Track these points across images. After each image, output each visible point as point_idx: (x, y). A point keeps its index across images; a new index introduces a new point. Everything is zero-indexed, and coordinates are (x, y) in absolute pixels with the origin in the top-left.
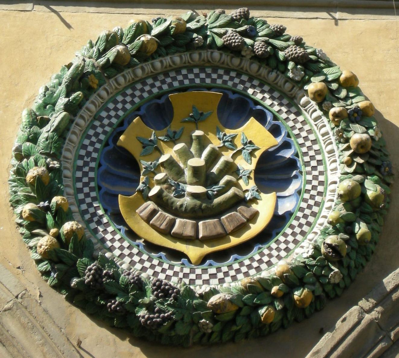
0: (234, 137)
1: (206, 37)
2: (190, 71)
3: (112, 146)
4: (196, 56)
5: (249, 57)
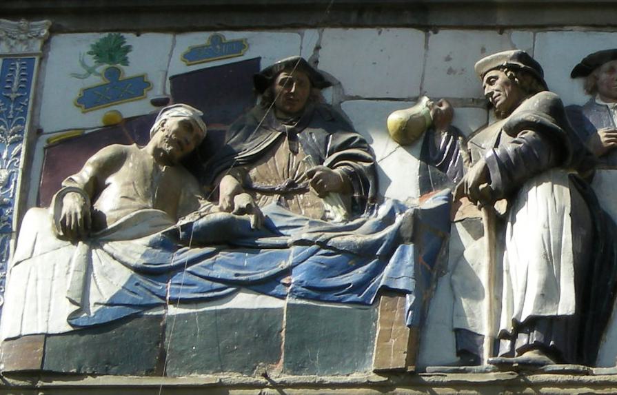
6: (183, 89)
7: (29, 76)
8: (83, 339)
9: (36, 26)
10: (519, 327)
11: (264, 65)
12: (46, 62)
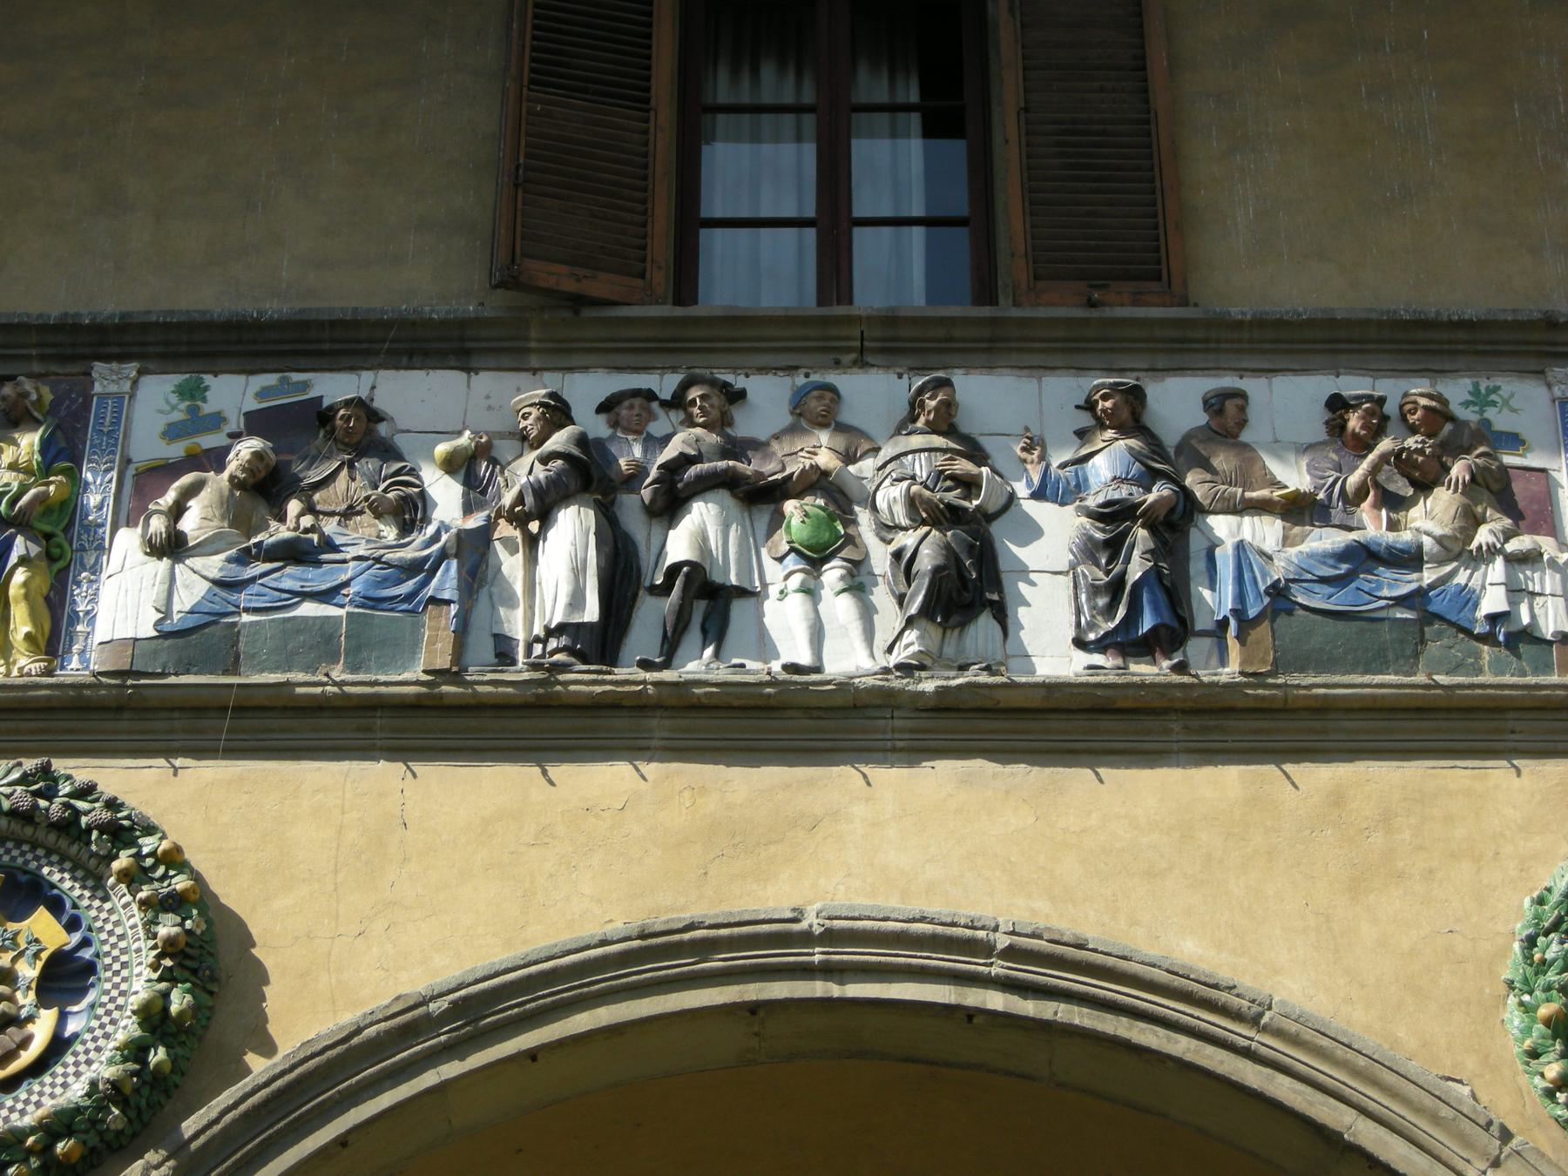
0: (16, 934)
5: (44, 824)
6: (256, 423)
8: (167, 643)
10: (550, 632)
11: (326, 403)
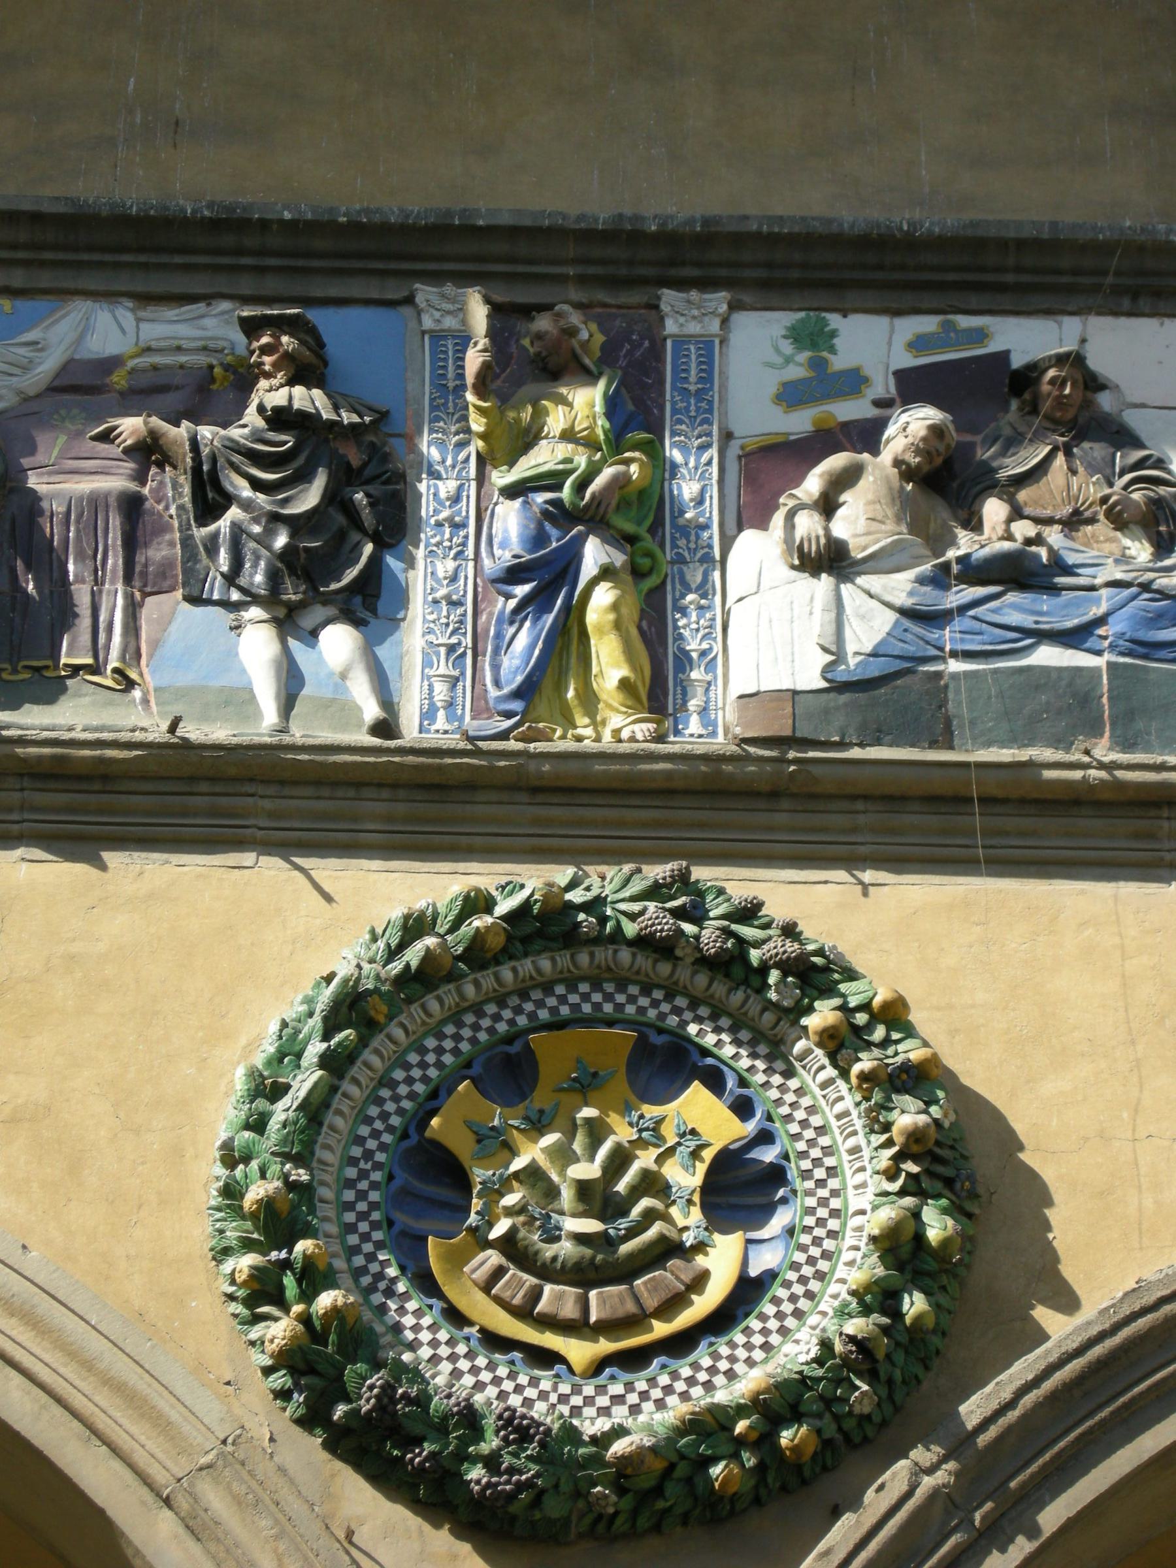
0: (660, 1121)
1: (603, 920)
2: (572, 988)
3: (414, 1138)
4: (583, 958)
5: (689, 960)
6: (913, 387)
7: (711, 363)
8: (844, 698)
9: (711, 300)
11: (1017, 362)
12: (728, 346)
